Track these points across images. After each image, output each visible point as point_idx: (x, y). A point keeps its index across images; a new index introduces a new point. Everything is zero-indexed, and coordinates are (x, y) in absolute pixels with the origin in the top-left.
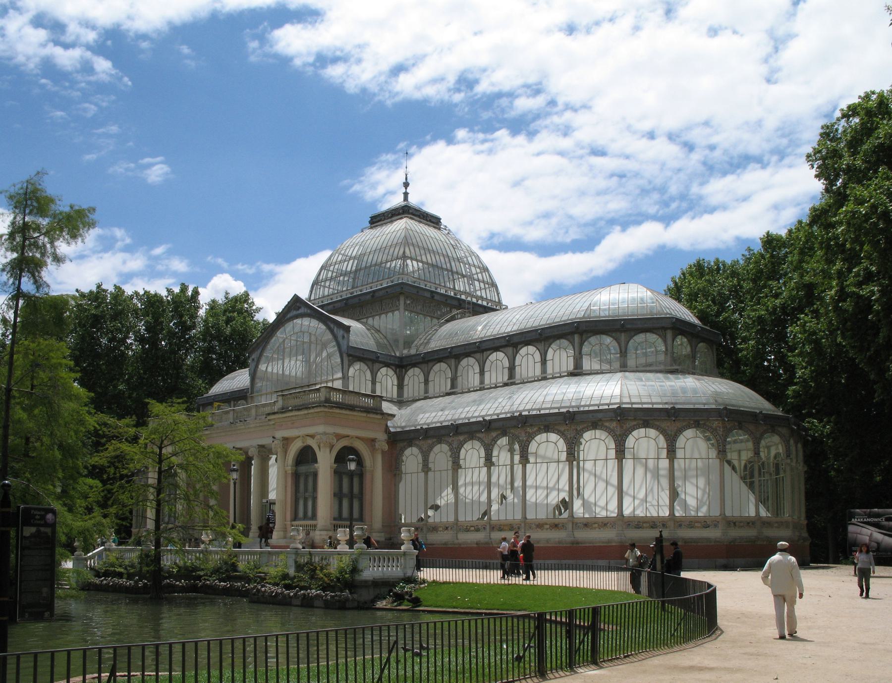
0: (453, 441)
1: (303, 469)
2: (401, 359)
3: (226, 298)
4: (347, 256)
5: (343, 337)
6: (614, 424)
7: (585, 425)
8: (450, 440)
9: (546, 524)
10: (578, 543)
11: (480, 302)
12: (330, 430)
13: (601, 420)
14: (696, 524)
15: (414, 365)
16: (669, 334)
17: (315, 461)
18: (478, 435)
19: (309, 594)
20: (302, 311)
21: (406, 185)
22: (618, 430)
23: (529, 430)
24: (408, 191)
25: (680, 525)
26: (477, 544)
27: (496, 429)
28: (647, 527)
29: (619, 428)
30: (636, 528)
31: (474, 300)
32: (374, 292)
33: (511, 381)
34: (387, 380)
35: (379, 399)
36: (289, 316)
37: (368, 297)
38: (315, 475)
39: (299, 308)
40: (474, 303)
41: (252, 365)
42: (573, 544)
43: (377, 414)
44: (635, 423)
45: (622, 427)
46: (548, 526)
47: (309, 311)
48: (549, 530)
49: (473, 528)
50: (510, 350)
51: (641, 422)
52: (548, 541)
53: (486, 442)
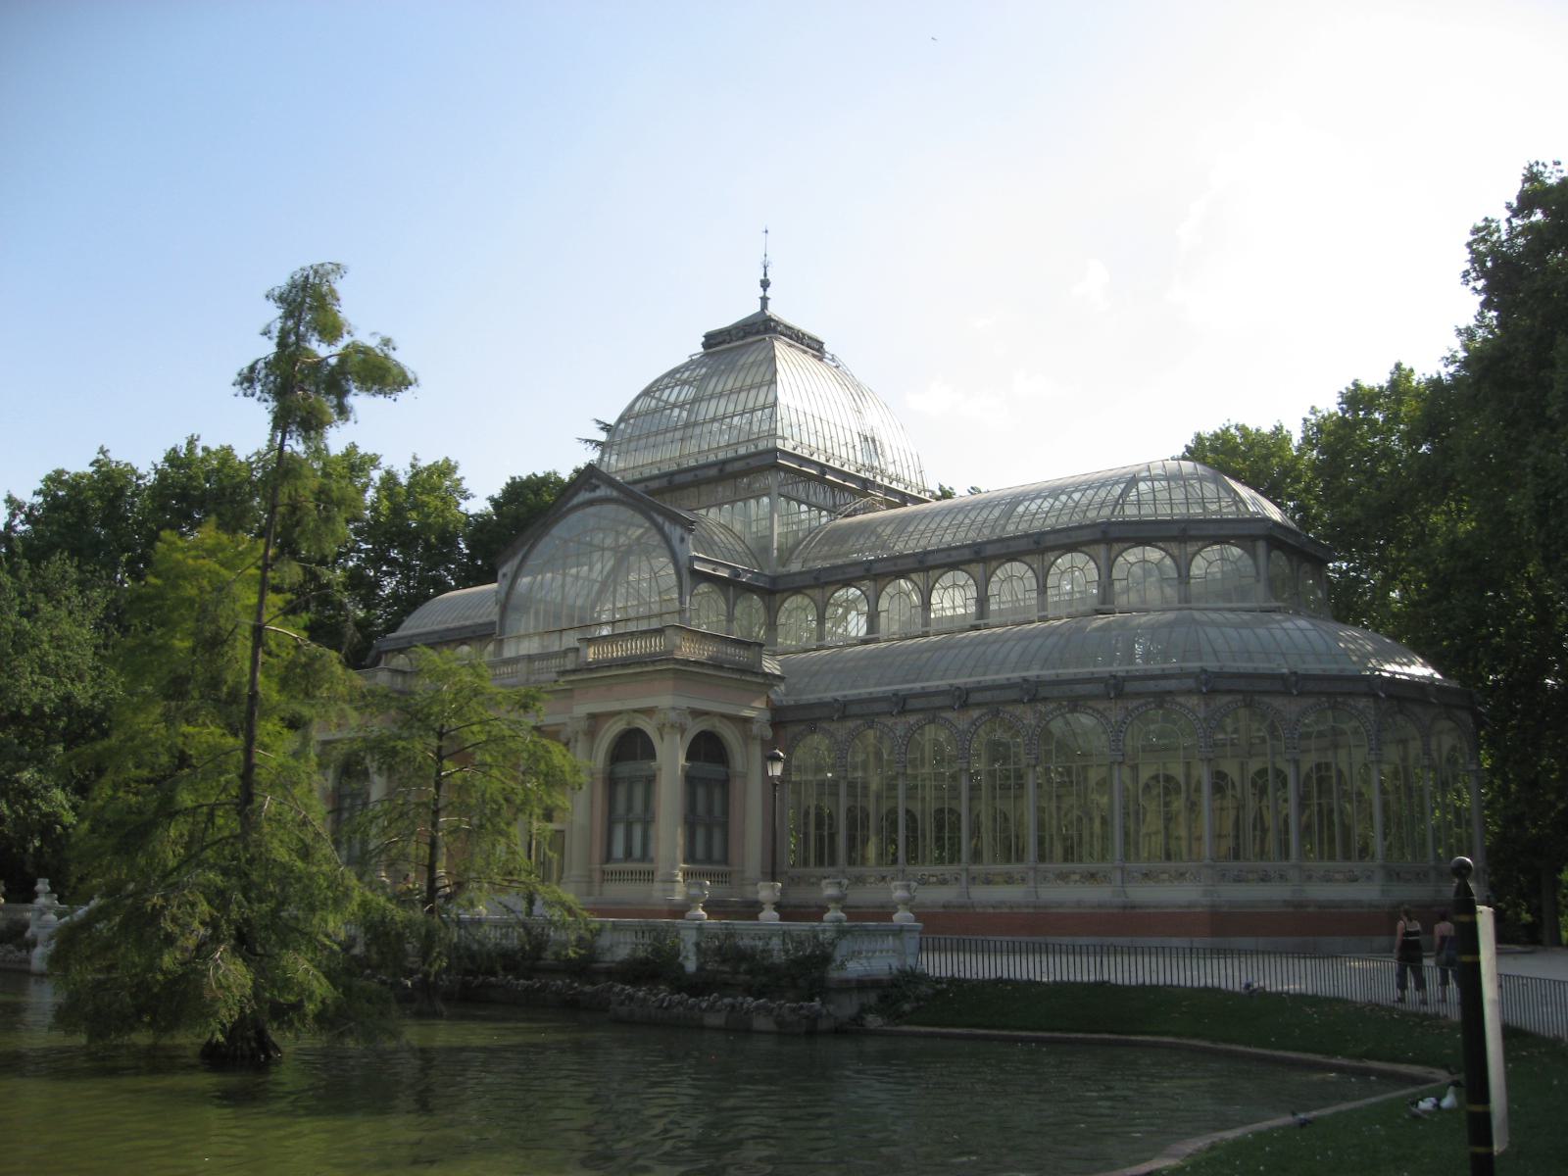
0: (896, 724)
1: (625, 769)
2: (774, 579)
3: (413, 466)
4: (666, 402)
5: (682, 540)
6: (1194, 701)
7: (1142, 701)
8: (890, 722)
9: (1074, 873)
10: (1133, 907)
11: (894, 485)
12: (684, 703)
13: (1170, 693)
14: (1337, 876)
15: (797, 590)
16: (1261, 547)
17: (650, 753)
18: (943, 715)
19: (742, 1004)
20: (602, 492)
21: (765, 284)
23: (1041, 707)
24: (768, 294)
25: (1310, 878)
26: (944, 907)
27: (978, 705)
29: (1203, 707)
30: (1235, 881)
31: (886, 482)
32: (724, 462)
33: (986, 621)
34: (749, 617)
36: (575, 501)
37: (713, 472)
38: (650, 781)
39: (597, 487)
40: (887, 488)
41: (506, 583)
42: (1125, 907)
43: (756, 674)
44: (1227, 699)
45: (1207, 705)
46: (1077, 877)
47: (615, 494)
49: (935, 879)
50: (978, 569)
51: (1240, 697)
52: (1079, 904)
53: (960, 727)
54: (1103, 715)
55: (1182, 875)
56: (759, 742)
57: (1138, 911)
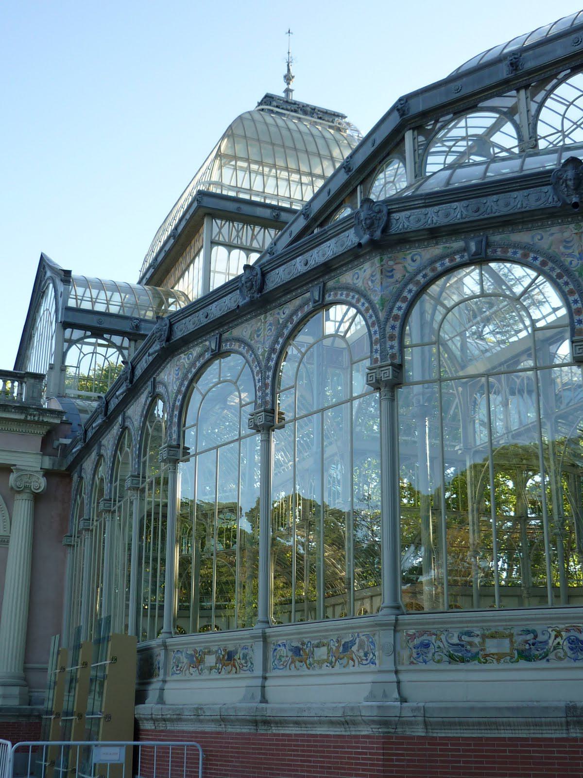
7: (297, 302)
9: (210, 653)
10: (266, 722)
21: (288, 78)
22: (378, 288)
23: (184, 360)
24: (290, 87)
28: (499, 657)
29: (378, 276)
30: (452, 659)
35: (32, 381)
44: (436, 250)
45: (387, 273)
46: (211, 660)
48: (214, 674)
51: (459, 244)
54: (250, 347)
55: (347, 647)
56: (25, 496)
57: (274, 730)
